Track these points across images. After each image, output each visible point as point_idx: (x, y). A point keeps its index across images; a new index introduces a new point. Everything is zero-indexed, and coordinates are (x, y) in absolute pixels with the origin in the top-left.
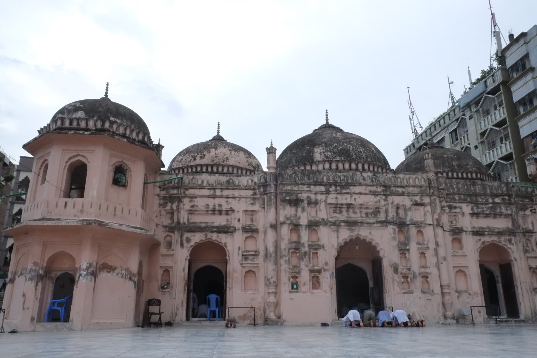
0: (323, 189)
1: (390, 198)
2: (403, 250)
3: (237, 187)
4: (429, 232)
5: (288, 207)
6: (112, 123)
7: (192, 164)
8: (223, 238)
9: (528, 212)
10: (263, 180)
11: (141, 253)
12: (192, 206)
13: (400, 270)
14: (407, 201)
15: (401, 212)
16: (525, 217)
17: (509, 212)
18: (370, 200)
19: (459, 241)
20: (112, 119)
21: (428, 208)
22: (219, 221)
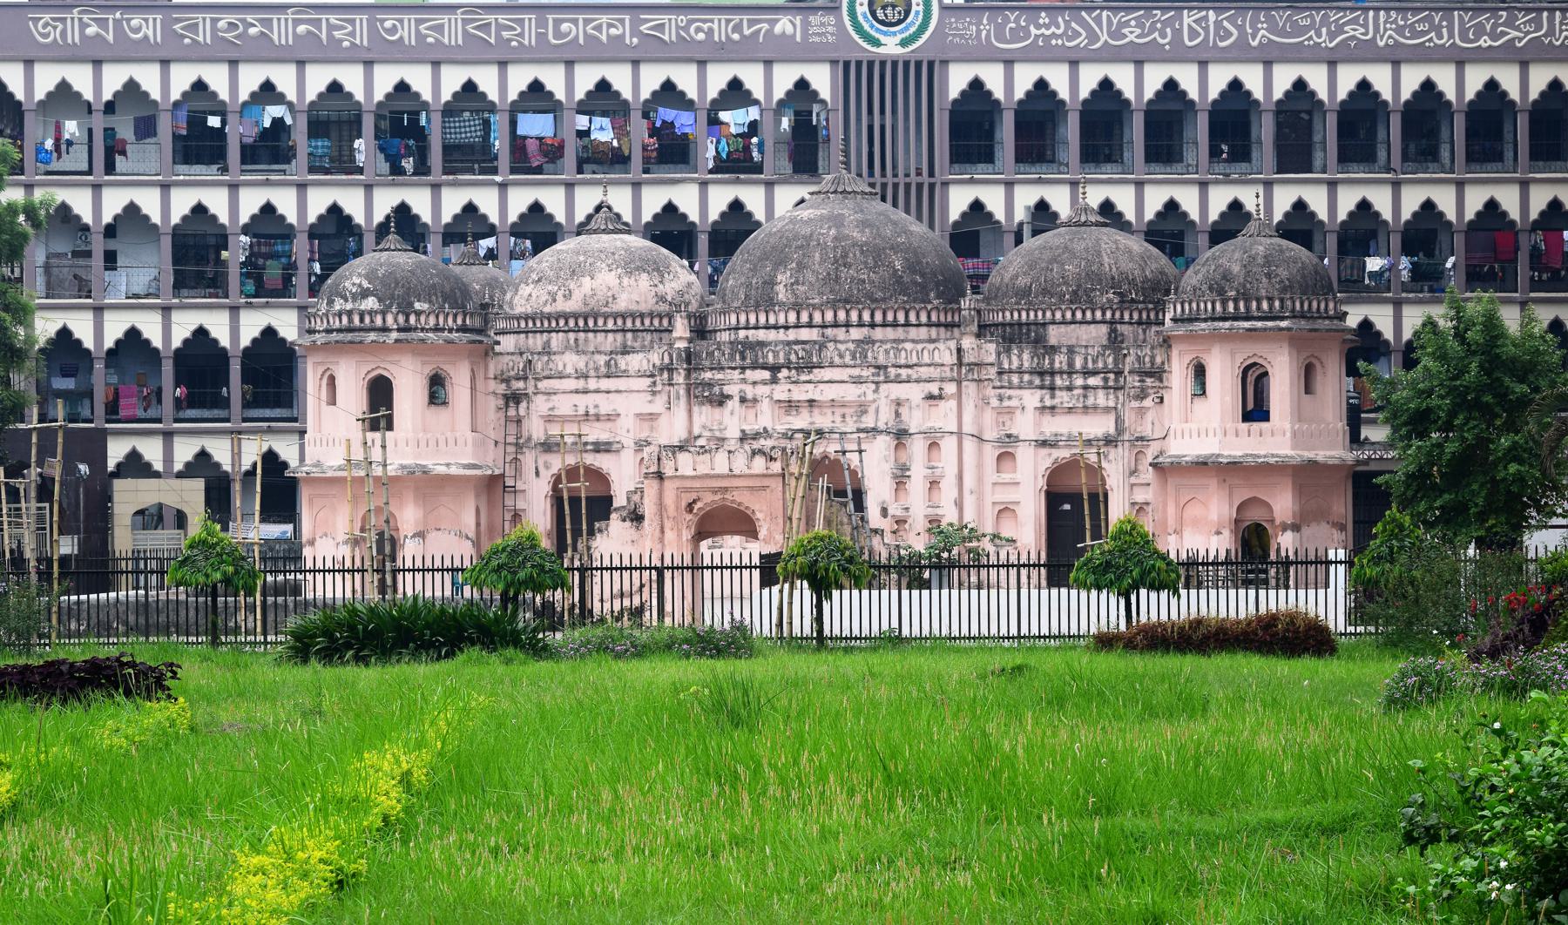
0: (766, 375)
1: (883, 387)
2: (901, 478)
3: (625, 374)
4: (949, 445)
5: (707, 409)
6: (418, 313)
7: (547, 309)
8: (602, 462)
9: (1148, 402)
10: (667, 360)
11: (477, 496)
12: (552, 409)
13: (891, 512)
14: (914, 393)
15: (904, 411)
16: (1141, 412)
17: (1111, 404)
18: (851, 393)
19: (1011, 455)
20: (417, 306)
21: (953, 403)
22: (595, 433)
